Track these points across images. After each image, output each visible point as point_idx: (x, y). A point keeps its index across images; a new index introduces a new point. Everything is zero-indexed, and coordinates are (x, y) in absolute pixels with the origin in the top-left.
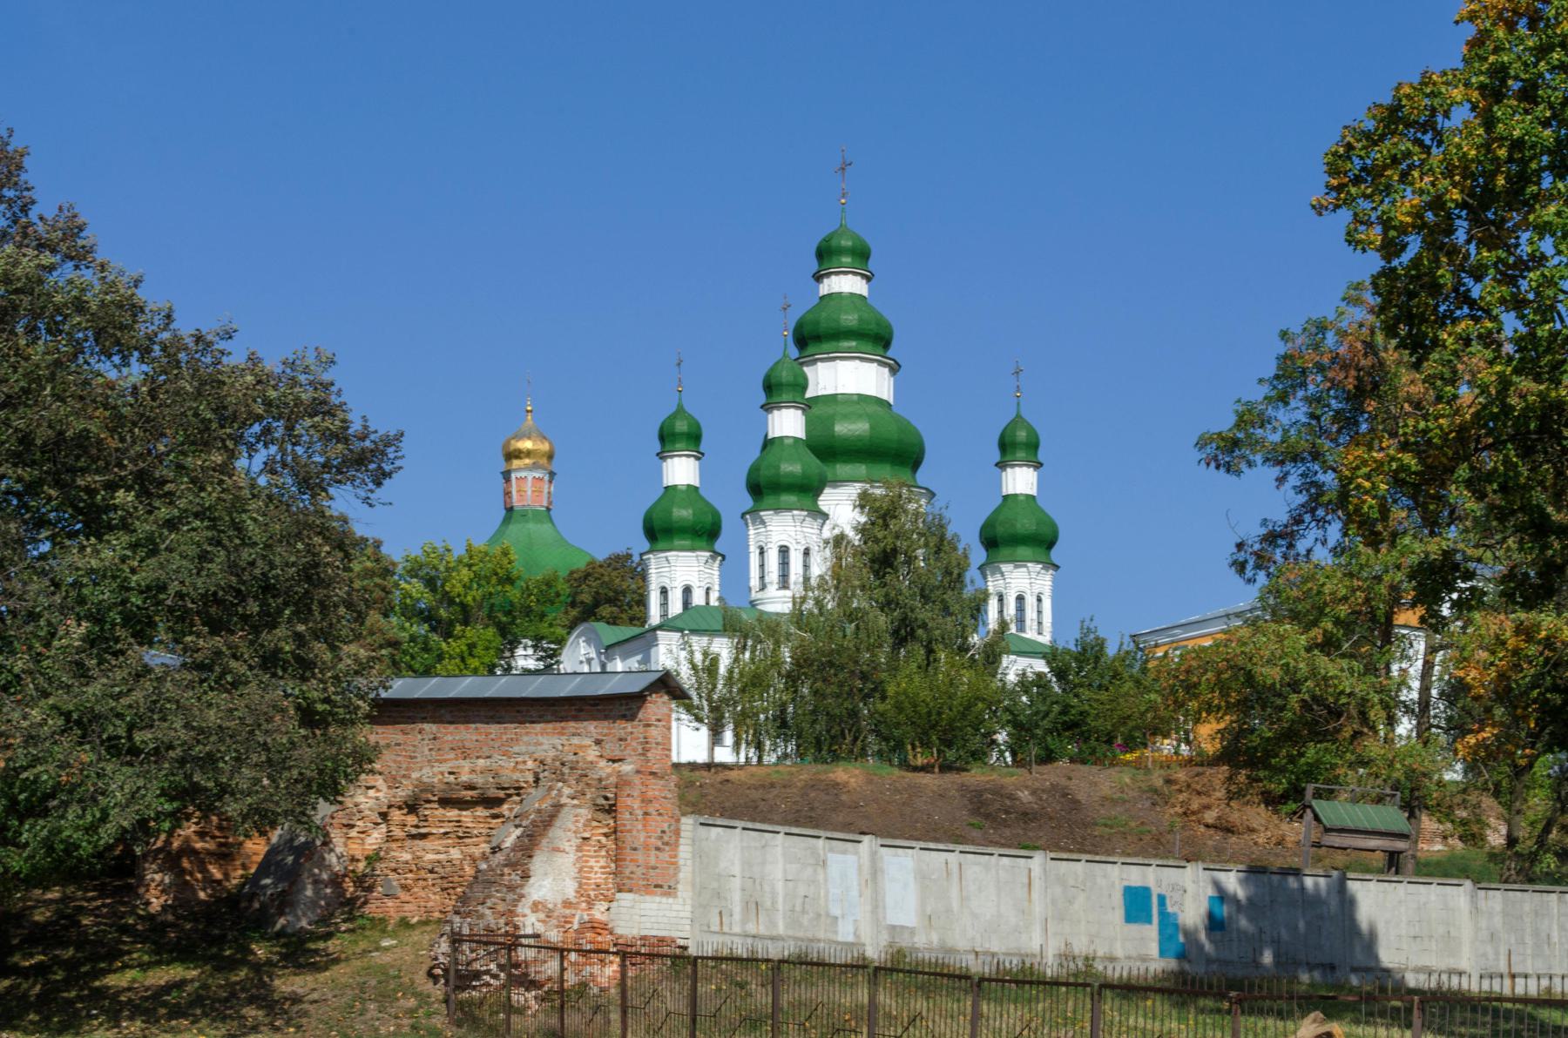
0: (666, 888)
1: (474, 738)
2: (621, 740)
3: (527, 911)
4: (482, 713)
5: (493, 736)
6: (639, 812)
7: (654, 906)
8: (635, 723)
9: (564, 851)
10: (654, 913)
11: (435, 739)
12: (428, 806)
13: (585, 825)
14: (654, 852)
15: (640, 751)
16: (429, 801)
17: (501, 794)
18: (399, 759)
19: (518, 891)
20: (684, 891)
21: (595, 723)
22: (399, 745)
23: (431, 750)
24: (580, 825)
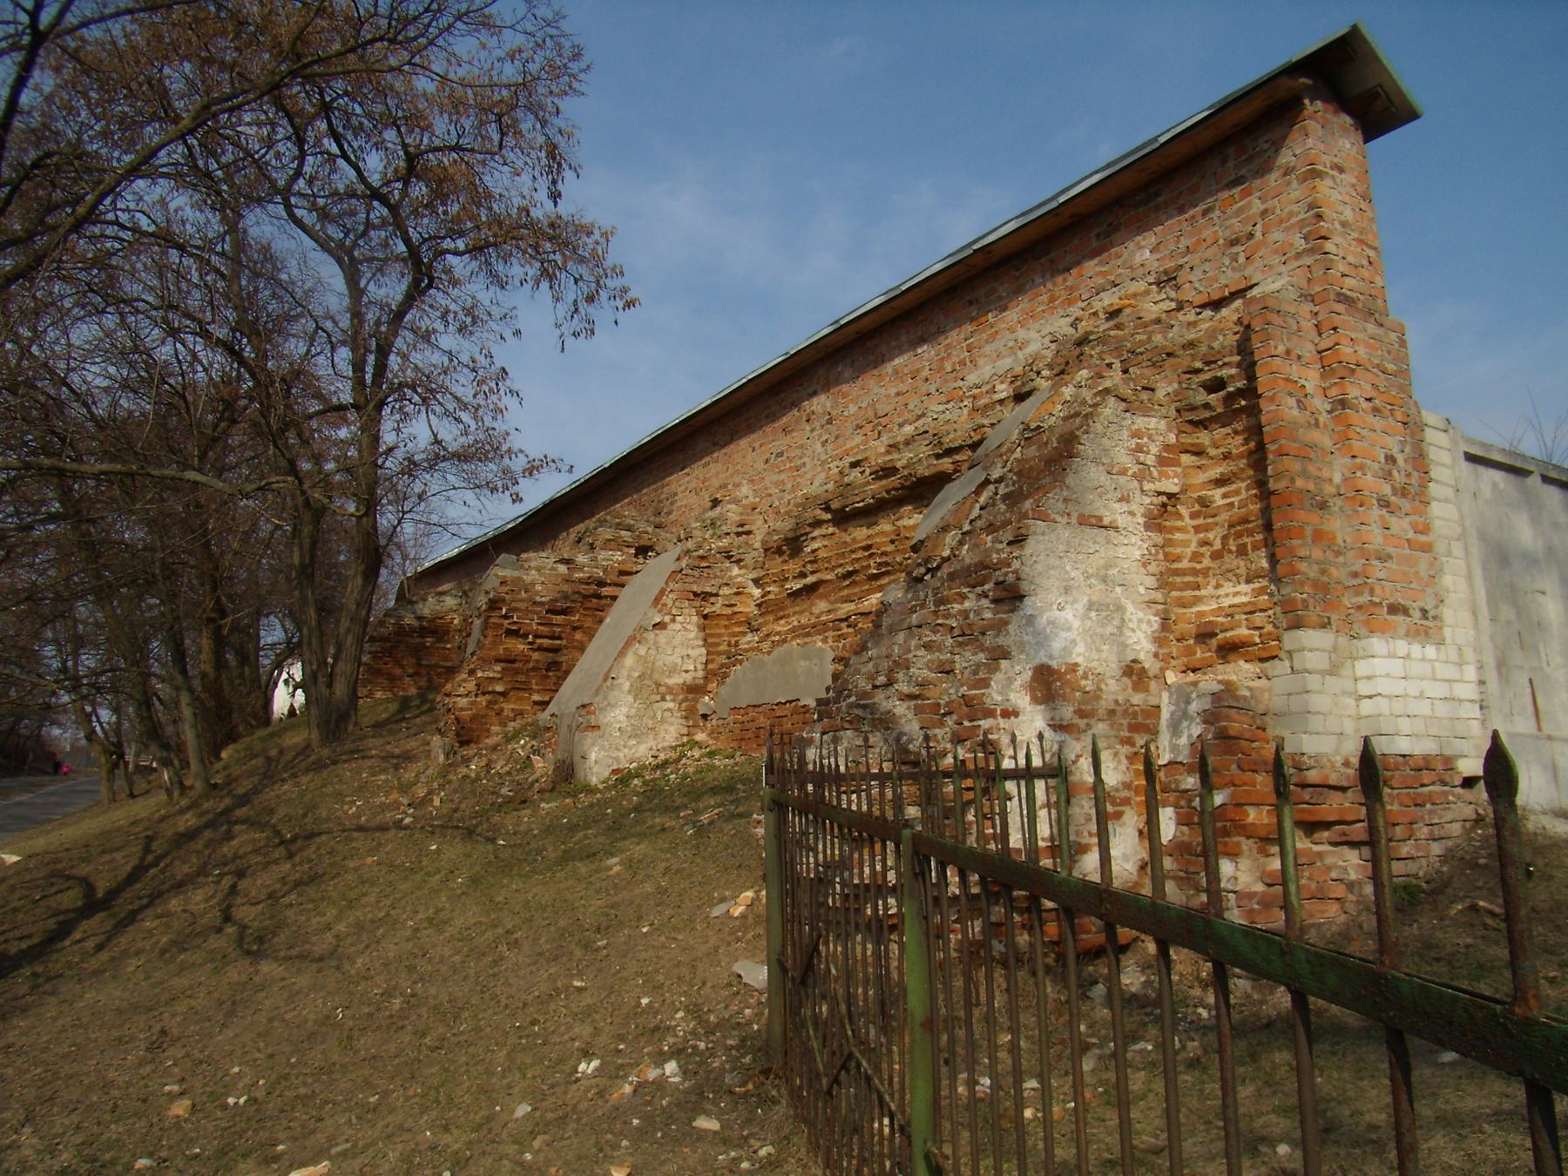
0: (1417, 614)
1: (893, 391)
2: (1234, 242)
3: (1022, 700)
4: (904, 338)
5: (926, 373)
6: (1320, 404)
7: (1396, 666)
8: (1273, 178)
9: (1113, 527)
10: (1399, 687)
11: (830, 422)
12: (816, 533)
13: (1162, 461)
14: (1376, 512)
15: (1300, 244)
16: (817, 523)
17: (946, 464)
18: (783, 477)
19: (988, 641)
20: (1458, 623)
21: (1149, 239)
22: (780, 454)
23: (824, 444)
24: (1150, 460)
